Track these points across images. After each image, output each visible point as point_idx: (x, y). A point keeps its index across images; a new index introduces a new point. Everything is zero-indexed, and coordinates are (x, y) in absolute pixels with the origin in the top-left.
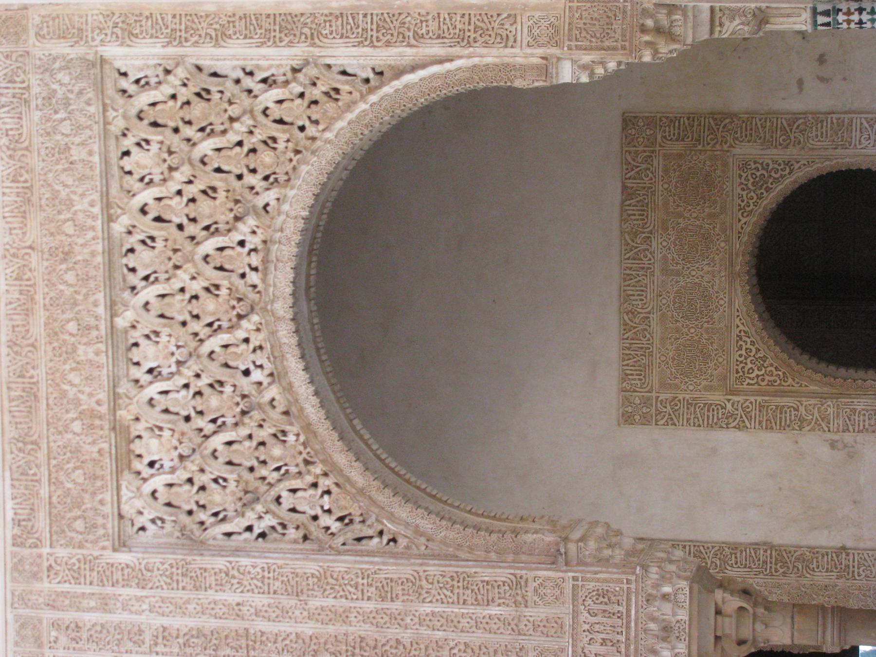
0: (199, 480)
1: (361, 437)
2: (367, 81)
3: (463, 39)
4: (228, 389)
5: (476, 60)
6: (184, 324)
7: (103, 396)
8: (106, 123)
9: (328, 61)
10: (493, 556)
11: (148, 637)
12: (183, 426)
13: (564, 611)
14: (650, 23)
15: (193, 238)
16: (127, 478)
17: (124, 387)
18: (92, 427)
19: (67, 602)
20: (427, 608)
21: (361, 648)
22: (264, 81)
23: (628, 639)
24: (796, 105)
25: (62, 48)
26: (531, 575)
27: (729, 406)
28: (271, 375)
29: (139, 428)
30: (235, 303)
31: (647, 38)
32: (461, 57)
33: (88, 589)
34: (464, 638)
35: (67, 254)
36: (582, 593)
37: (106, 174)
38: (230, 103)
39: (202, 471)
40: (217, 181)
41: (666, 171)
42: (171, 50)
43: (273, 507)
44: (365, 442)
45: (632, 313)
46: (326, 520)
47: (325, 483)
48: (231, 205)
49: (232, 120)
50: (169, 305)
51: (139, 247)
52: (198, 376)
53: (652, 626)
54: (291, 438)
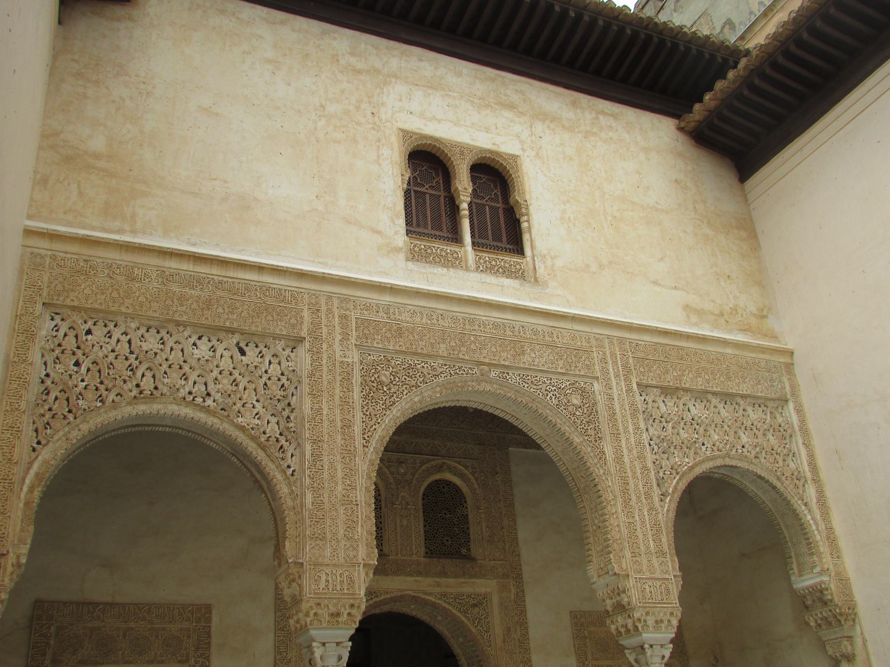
3: (828, 538)
5: (820, 543)
7: (687, 386)
9: (806, 485)
11: (609, 391)
19: (614, 360)
20: (646, 513)
21: (625, 483)
23: (654, 603)
25: (788, 389)
26: (668, 559)
29: (675, 397)
30: (725, 441)
32: (820, 536)
34: (638, 528)
35: (729, 378)
36: (666, 582)
42: (796, 428)
48: (754, 443)
52: (697, 425)
53: (662, 614)
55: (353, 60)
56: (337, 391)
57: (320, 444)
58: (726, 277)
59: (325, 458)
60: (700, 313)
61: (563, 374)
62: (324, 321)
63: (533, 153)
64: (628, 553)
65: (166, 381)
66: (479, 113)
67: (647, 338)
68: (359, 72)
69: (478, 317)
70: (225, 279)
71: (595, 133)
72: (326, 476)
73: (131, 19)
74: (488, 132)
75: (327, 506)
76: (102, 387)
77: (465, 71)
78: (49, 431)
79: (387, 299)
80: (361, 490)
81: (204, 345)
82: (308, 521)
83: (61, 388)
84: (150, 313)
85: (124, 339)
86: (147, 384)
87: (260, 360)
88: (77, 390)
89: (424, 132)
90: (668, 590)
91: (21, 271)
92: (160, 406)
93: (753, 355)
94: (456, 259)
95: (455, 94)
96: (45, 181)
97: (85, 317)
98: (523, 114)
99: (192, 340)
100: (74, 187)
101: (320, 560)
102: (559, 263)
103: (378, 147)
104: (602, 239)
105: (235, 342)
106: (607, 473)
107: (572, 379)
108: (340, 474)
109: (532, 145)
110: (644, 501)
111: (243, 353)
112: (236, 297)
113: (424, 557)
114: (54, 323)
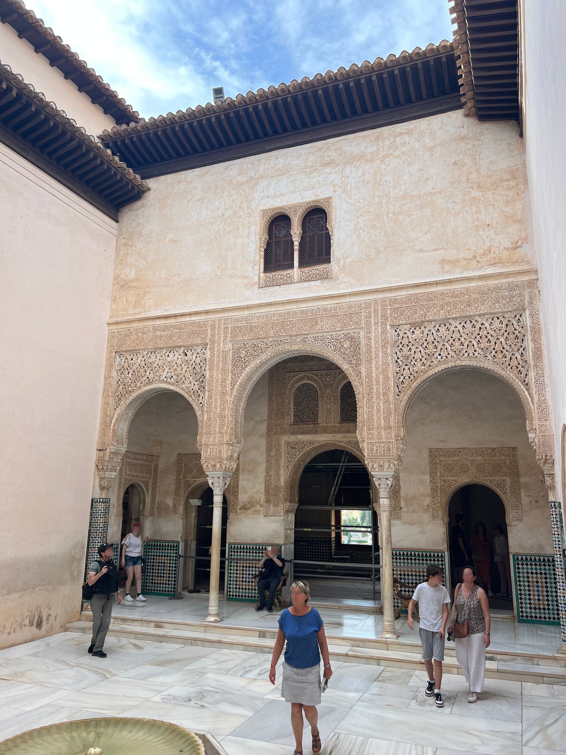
0: (410, 345)
1: (424, 385)
2: (525, 381)
3: (539, 406)
4: (435, 350)
5: (533, 411)
6: (452, 337)
7: (431, 318)
8: (507, 312)
10: (396, 421)
11: (369, 335)
12: (424, 339)
13: (384, 440)
14: (548, 458)
15: (476, 338)
16: (409, 326)
17: (433, 323)
18: (422, 316)
22: (522, 353)
24: (522, 494)
26: (393, 431)
27: (436, 478)
28: (440, 361)
29: (423, 328)
31: (544, 457)
32: (534, 406)
33: (380, 319)
34: (375, 414)
36: (389, 444)
37: (491, 314)
38: (515, 345)
39: (413, 345)
40: (493, 343)
41: (501, 460)
42: (529, 328)
43: (404, 364)
44: (423, 386)
45: (460, 452)
46: (402, 378)
47: (412, 377)
48: (486, 347)
49: (510, 346)
50: (456, 333)
51: (472, 324)
52: (438, 342)
54: (423, 367)
55: (239, 178)
56: (220, 365)
57: (212, 391)
58: (486, 226)
59: (213, 398)
60: (454, 263)
61: (340, 331)
62: (216, 333)
63: (342, 190)
64: (365, 429)
65: (157, 374)
66: (309, 178)
67: (404, 293)
68: (243, 184)
69: (293, 310)
70: (177, 324)
71: (391, 154)
72: (213, 406)
73: (143, 206)
74: (313, 189)
75: (213, 419)
76: (136, 381)
77: (303, 153)
78: (120, 402)
79: (246, 313)
80: (228, 410)
81: (171, 355)
82: (204, 427)
83: (123, 384)
84: (149, 347)
85: (143, 359)
86: (151, 376)
87: (191, 357)
88: (129, 384)
89: (274, 207)
90: (389, 449)
91: (108, 340)
92: (155, 385)
93: (496, 282)
94: (289, 277)
95: (295, 172)
96: (115, 299)
97: (130, 354)
98: (338, 165)
99: (167, 354)
100: (125, 298)
101: (208, 443)
102: (348, 260)
103: (249, 227)
104: (382, 234)
105: (182, 351)
106: (361, 384)
107: (345, 332)
108: (219, 404)
109: (341, 185)
110: (382, 397)
111: (186, 355)
112: (181, 331)
113: (339, 423)
114: (120, 358)
